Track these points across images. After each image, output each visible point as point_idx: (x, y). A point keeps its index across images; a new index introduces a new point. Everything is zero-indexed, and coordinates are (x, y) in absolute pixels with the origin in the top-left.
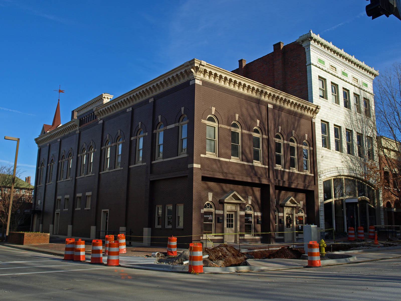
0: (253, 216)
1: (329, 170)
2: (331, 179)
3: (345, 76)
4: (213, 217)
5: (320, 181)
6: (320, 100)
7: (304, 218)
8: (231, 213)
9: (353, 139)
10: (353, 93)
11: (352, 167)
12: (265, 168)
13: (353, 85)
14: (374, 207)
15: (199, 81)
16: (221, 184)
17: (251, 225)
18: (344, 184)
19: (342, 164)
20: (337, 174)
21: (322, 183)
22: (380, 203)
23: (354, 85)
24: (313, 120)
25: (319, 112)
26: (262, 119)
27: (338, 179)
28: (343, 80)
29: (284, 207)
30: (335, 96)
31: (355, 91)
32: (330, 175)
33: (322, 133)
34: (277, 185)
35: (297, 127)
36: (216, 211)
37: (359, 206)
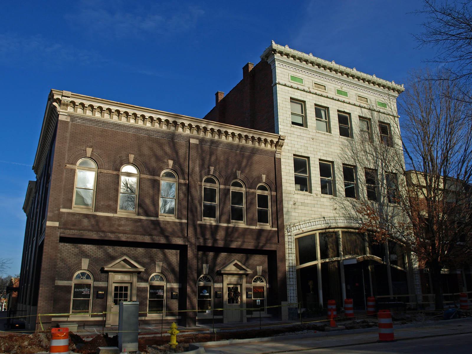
0: (165, 288)
1: (309, 222)
2: (316, 233)
3: (341, 96)
4: (90, 290)
5: (290, 237)
6: (292, 129)
7: (265, 289)
8: (124, 285)
9: (358, 177)
10: (358, 116)
11: (356, 215)
12: (181, 224)
13: (359, 106)
14: (403, 269)
15: (65, 117)
16: (79, 245)
17: (163, 300)
18: (341, 240)
19: (334, 212)
20: (323, 226)
21: (293, 238)
22: (412, 263)
23: (360, 106)
24: (277, 156)
25: (284, 144)
26: (178, 158)
27: (329, 232)
28: (338, 100)
29: (224, 276)
30: (326, 122)
31: (361, 114)
32: (310, 227)
33: (321, 176)
34: (202, 244)
35: (246, 166)
36: (95, 282)
37: (371, 268)
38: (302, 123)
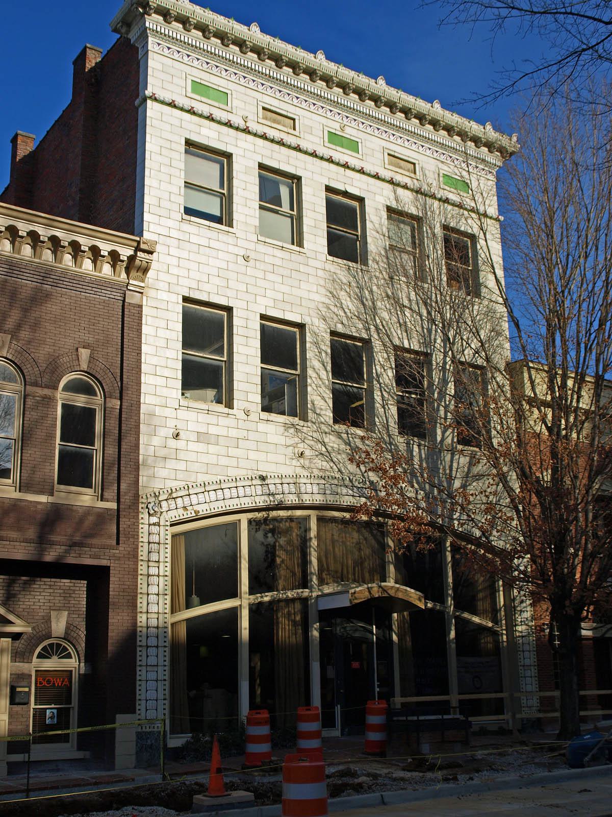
2: (240, 521)
5: (154, 529)
6: (186, 227)
20: (261, 501)
21: (165, 534)
22: (515, 607)
23: (391, 182)
24: (132, 298)
25: (154, 265)
28: (330, 160)
30: (291, 217)
32: (221, 503)
38: (218, 214)
